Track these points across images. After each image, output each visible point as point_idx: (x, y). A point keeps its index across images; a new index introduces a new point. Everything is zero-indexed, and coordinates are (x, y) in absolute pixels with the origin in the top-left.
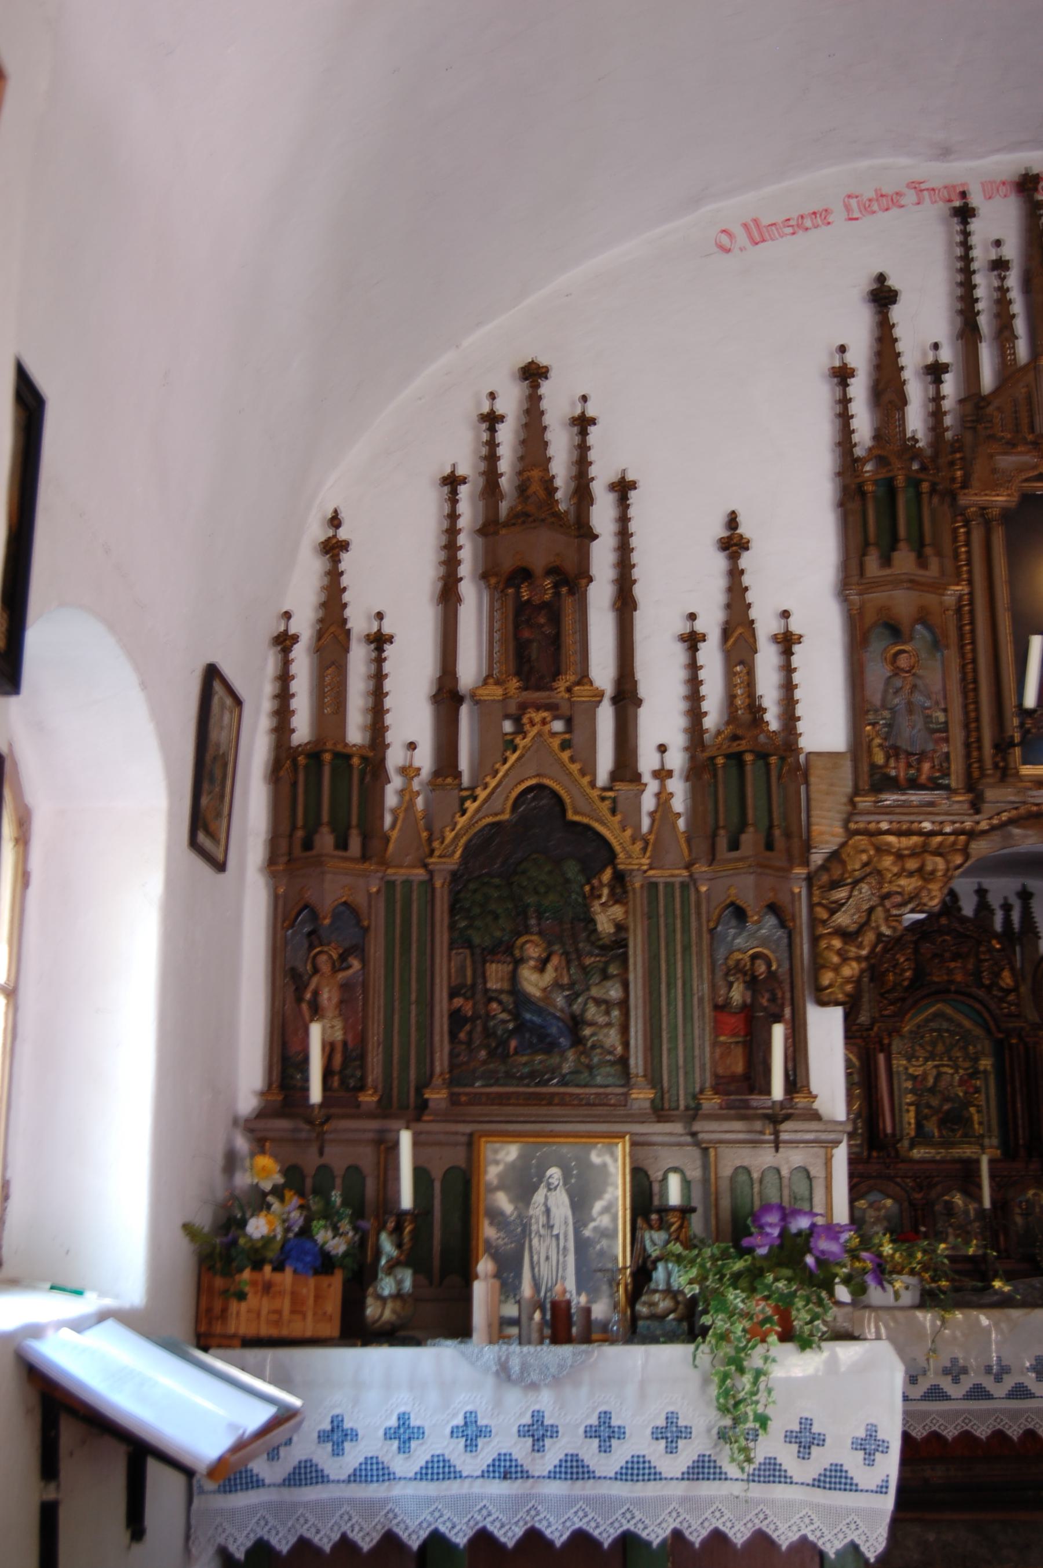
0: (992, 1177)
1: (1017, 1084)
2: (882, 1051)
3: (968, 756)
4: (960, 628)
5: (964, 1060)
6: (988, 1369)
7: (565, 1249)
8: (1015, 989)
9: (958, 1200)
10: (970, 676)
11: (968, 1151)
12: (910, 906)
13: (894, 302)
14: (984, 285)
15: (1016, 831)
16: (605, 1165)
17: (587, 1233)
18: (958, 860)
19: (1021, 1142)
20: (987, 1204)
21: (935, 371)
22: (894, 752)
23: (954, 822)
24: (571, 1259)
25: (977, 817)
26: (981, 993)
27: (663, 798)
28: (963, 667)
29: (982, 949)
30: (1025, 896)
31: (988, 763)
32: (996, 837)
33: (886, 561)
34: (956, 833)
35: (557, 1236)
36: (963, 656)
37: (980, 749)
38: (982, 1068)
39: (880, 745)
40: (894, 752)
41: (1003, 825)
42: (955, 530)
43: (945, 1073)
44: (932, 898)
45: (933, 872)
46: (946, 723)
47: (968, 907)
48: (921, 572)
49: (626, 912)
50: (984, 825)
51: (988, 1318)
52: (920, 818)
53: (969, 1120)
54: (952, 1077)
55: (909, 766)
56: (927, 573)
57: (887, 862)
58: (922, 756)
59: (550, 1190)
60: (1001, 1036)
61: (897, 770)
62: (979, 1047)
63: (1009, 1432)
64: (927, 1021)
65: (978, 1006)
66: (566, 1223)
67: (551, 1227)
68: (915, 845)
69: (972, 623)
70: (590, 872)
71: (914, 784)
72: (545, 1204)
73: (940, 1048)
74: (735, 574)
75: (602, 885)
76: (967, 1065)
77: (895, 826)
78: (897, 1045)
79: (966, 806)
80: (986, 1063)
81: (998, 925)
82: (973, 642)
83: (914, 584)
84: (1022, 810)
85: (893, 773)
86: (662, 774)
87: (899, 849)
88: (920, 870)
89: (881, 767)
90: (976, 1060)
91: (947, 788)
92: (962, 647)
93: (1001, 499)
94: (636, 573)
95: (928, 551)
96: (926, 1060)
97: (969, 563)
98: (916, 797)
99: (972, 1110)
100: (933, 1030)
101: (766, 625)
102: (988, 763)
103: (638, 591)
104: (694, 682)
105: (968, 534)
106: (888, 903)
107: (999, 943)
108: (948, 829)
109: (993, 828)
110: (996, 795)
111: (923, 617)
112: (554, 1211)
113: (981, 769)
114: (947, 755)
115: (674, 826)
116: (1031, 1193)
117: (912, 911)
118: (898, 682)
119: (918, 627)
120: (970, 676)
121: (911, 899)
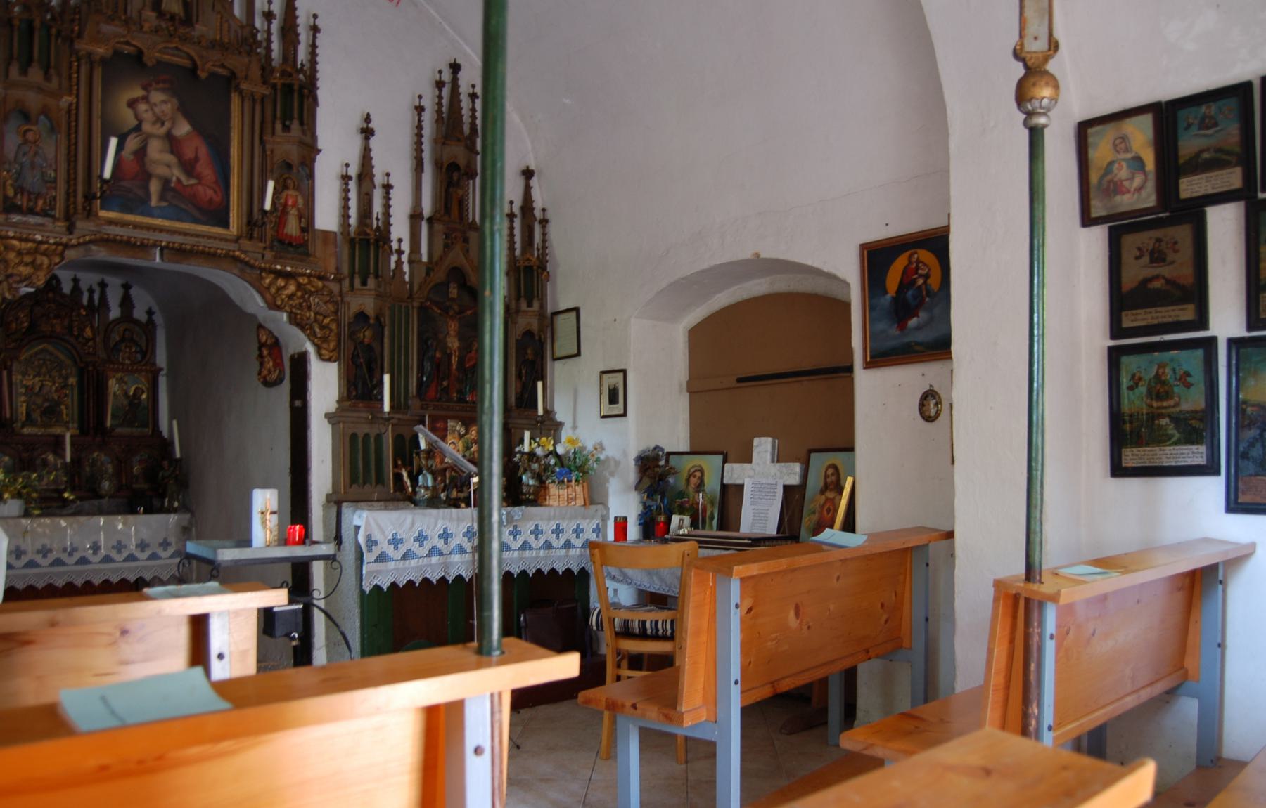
0: (72, 444)
1: (91, 393)
2: (5, 368)
3: (68, 200)
4: (69, 123)
5: (59, 378)
6: (65, 550)
8: (93, 339)
9: (51, 458)
10: (73, 153)
11: (58, 430)
12: (25, 283)
15: (94, 248)
18: (57, 260)
19: (91, 425)
20: (68, 459)
22: (20, 190)
23: (56, 238)
25: (71, 237)
26: (72, 340)
28: (69, 147)
29: (74, 314)
30: (103, 285)
31: (80, 207)
32: (81, 250)
33: (24, 72)
34: (57, 244)
36: (69, 140)
37: (75, 196)
38: (70, 383)
39: (12, 185)
40: (20, 190)
41: (85, 243)
42: (71, 63)
43: (47, 385)
44: (39, 280)
45: (41, 265)
46: (56, 178)
47: (67, 288)
50: (74, 242)
51: (65, 522)
52: (35, 232)
53: (60, 413)
54: (51, 387)
55: (29, 200)
57: (12, 255)
58: (38, 195)
60: (82, 365)
61: (21, 201)
62: (69, 371)
63: (76, 583)
64: (36, 353)
65: (69, 347)
68: (30, 248)
69: (77, 120)
71: (31, 211)
73: (44, 370)
76: (61, 380)
77: (18, 235)
78: (15, 366)
79: (64, 229)
80: (72, 380)
81: (85, 301)
82: (76, 132)
83: (40, 90)
84: (98, 236)
85: (19, 203)
87: (20, 249)
88: (33, 263)
90: (66, 378)
91: (53, 217)
92: (69, 135)
93: (101, 51)
95: (52, 71)
96: (35, 376)
97: (78, 84)
98: (32, 220)
99: (63, 407)
100: (39, 360)
102: (80, 207)
105: (79, 66)
106: (11, 281)
107: (84, 311)
108: (52, 241)
109: (79, 244)
110: (82, 225)
111: (45, 111)
113: (75, 208)
114: (55, 198)
116: (95, 454)
117: (26, 286)
118: (26, 148)
119: (42, 117)
120: (73, 153)
121: (26, 279)
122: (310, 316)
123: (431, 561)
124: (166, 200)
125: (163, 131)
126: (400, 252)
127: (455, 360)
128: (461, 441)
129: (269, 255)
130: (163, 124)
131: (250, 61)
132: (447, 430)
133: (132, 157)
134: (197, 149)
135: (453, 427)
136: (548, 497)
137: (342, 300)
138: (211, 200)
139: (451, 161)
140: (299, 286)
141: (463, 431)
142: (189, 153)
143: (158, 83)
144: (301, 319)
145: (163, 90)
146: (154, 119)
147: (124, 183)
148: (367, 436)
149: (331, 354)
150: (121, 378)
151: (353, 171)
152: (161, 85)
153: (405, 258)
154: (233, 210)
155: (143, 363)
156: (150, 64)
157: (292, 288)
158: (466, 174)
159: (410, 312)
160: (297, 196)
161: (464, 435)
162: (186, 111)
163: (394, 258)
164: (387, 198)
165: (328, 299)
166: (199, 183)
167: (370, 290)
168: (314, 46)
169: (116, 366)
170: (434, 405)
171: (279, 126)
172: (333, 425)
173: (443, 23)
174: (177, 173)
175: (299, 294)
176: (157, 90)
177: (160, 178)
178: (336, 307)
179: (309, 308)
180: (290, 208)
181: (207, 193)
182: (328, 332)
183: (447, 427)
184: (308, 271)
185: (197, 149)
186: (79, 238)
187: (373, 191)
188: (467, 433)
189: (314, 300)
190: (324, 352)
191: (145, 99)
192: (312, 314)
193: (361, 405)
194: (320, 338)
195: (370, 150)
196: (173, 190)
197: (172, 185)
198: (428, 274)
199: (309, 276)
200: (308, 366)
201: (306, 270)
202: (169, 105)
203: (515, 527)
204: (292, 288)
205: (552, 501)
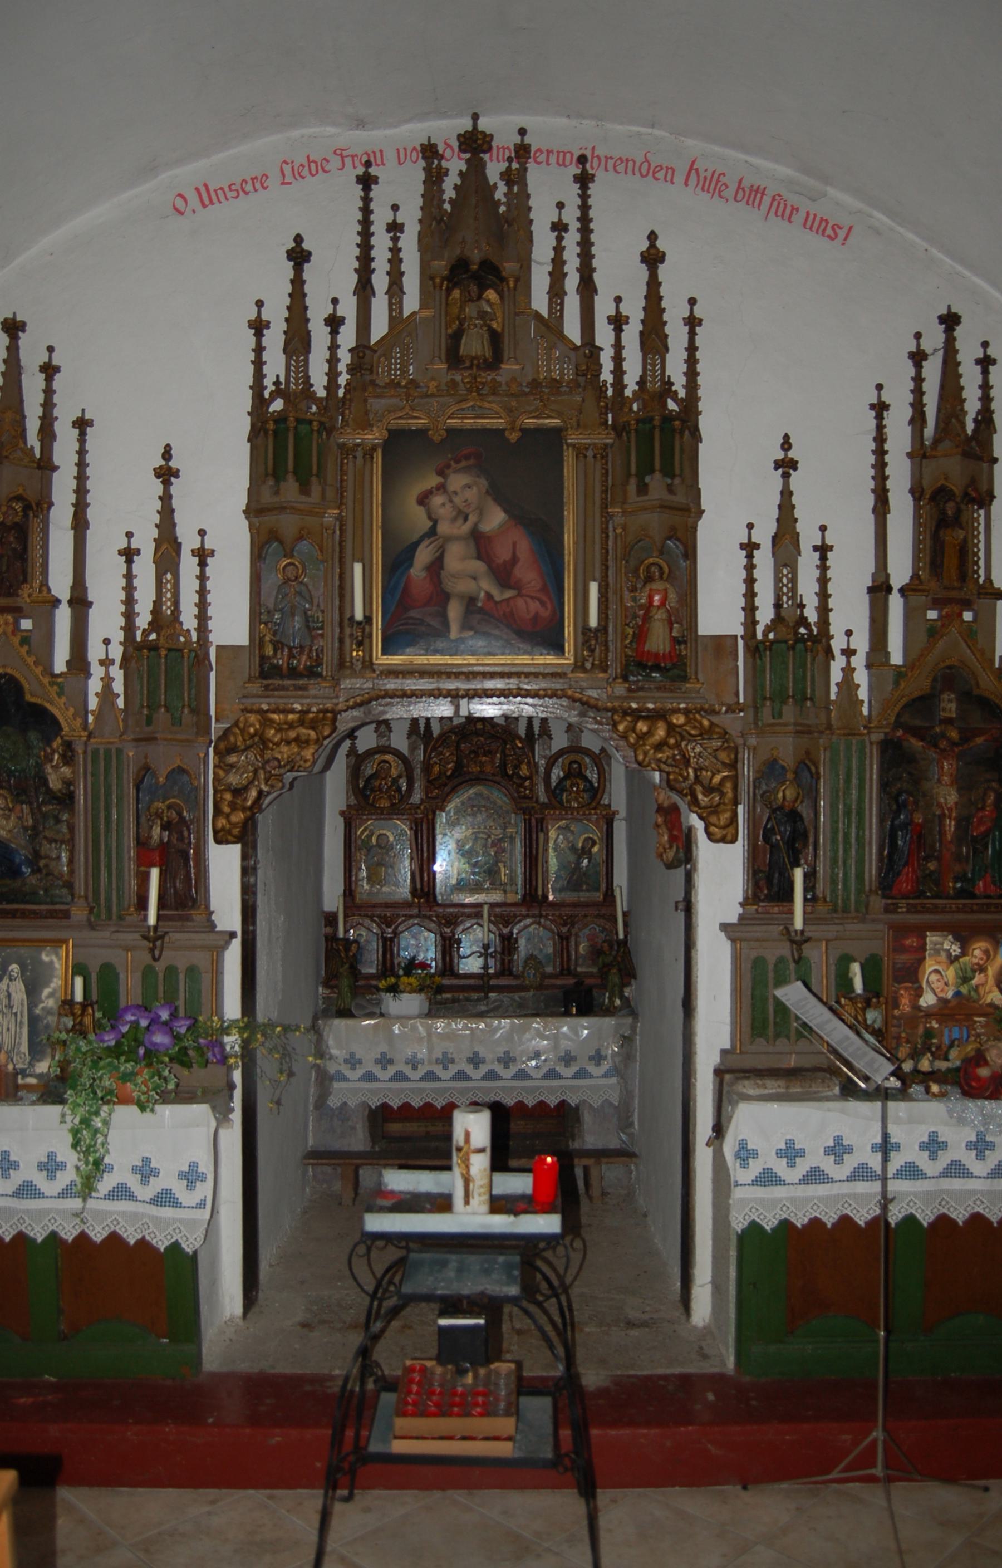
7: (21, 1022)
13: (308, 261)
14: (381, 243)
16: (52, 962)
17: (37, 1011)
21: (334, 323)
24: (25, 1031)
27: (107, 681)
34: (319, 711)
35: (16, 1014)
40: (278, 646)
48: (304, 498)
49: (73, 772)
52: (292, 701)
56: (309, 500)
59: (11, 980)
66: (22, 1004)
67: (10, 1007)
70: (48, 741)
72: (8, 991)
74: (166, 498)
75: (53, 752)
86: (106, 662)
89: (269, 658)
94: (89, 498)
101: (189, 541)
103: (91, 514)
104: (129, 589)
112: (13, 995)
115: (113, 704)
122: (688, 773)
124: (471, 628)
125: (466, 528)
126: (849, 653)
127: (950, 826)
128: (952, 968)
129: (620, 689)
130: (466, 519)
131: (583, 401)
132: (925, 950)
133: (424, 574)
134: (514, 545)
137: (745, 744)
138: (536, 617)
139: (939, 484)
140: (671, 728)
141: (956, 950)
142: (503, 554)
143: (458, 461)
144: (675, 780)
145: (466, 470)
146: (454, 513)
147: (413, 614)
148: (781, 960)
149: (724, 832)
150: (567, 828)
151: (764, 535)
152: (464, 464)
153: (859, 662)
154: (569, 626)
155: (594, 804)
156: (437, 438)
157: (661, 733)
158: (973, 501)
159: (867, 750)
160: (666, 590)
161: (957, 958)
162: (497, 494)
164: (823, 568)
165: (719, 744)
166: (519, 595)
167: (785, 725)
168: (692, 349)
169: (557, 812)
170: (908, 904)
171: (632, 487)
172: (733, 940)
174: (487, 585)
175: (672, 741)
176: (456, 471)
177: (461, 597)
178: (733, 756)
179: (687, 762)
180: (654, 610)
181: (529, 608)
182: (717, 798)
183: (925, 944)
184: (682, 706)
185: (514, 545)
186: (347, 701)
187: (796, 561)
188: (964, 954)
189: (694, 749)
190: (713, 829)
191: (442, 488)
192: (691, 770)
193: (776, 909)
194: (705, 808)
195: (791, 493)
196: (481, 611)
197: (480, 604)
198: (897, 683)
199: (686, 712)
200: (694, 848)
201: (679, 703)
202: (475, 489)
204: (661, 733)
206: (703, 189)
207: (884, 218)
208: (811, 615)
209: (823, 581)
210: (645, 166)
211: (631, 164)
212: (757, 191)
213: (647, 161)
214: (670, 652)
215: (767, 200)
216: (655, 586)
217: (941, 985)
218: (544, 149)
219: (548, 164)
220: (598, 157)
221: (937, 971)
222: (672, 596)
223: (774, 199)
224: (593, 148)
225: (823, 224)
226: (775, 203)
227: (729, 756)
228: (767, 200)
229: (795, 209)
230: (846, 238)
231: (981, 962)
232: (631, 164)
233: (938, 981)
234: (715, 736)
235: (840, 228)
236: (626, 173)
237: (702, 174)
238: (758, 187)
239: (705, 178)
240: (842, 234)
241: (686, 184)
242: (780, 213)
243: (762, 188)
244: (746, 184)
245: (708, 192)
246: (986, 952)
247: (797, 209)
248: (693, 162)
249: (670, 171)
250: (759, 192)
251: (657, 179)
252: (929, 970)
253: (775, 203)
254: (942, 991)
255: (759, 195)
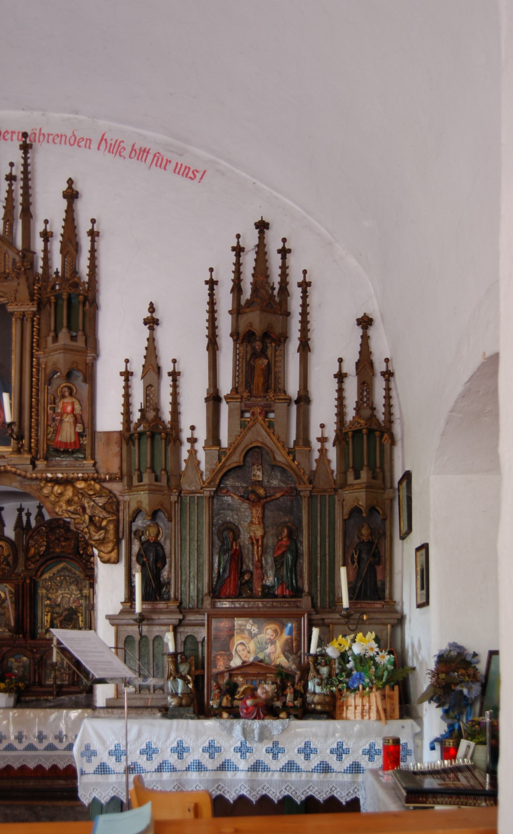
123: (162, 776)
135: (241, 626)
136: (345, 708)
163: (186, 447)
173: (258, 183)
175: (76, 499)
183: (234, 626)
203: (276, 744)
205: (350, 713)
206: (109, 152)
207: (227, 165)
208: (167, 417)
209: (175, 395)
210: (73, 139)
211: (64, 138)
212: (144, 151)
213: (74, 135)
214: (75, 442)
215: (150, 157)
216: (66, 400)
217: (245, 653)
218: (10, 131)
219: (12, 140)
220: (44, 135)
221: (242, 644)
222: (77, 406)
223: (155, 156)
224: (40, 129)
225: (187, 170)
226: (156, 158)
227: (112, 507)
228: (150, 157)
229: (168, 161)
230: (201, 179)
231: (272, 638)
232: (64, 138)
233: (243, 650)
234: (104, 495)
235: (197, 172)
236: (60, 143)
237: (109, 142)
238: (145, 149)
239: (111, 145)
240: (199, 175)
241: (99, 149)
242: (158, 164)
243: (147, 149)
244: (137, 147)
245: (113, 152)
246: (275, 631)
247: (170, 162)
248: (103, 135)
249: (88, 141)
250: (145, 151)
251: (80, 146)
252: (236, 643)
253: (156, 158)
254: (246, 657)
255: (145, 154)
